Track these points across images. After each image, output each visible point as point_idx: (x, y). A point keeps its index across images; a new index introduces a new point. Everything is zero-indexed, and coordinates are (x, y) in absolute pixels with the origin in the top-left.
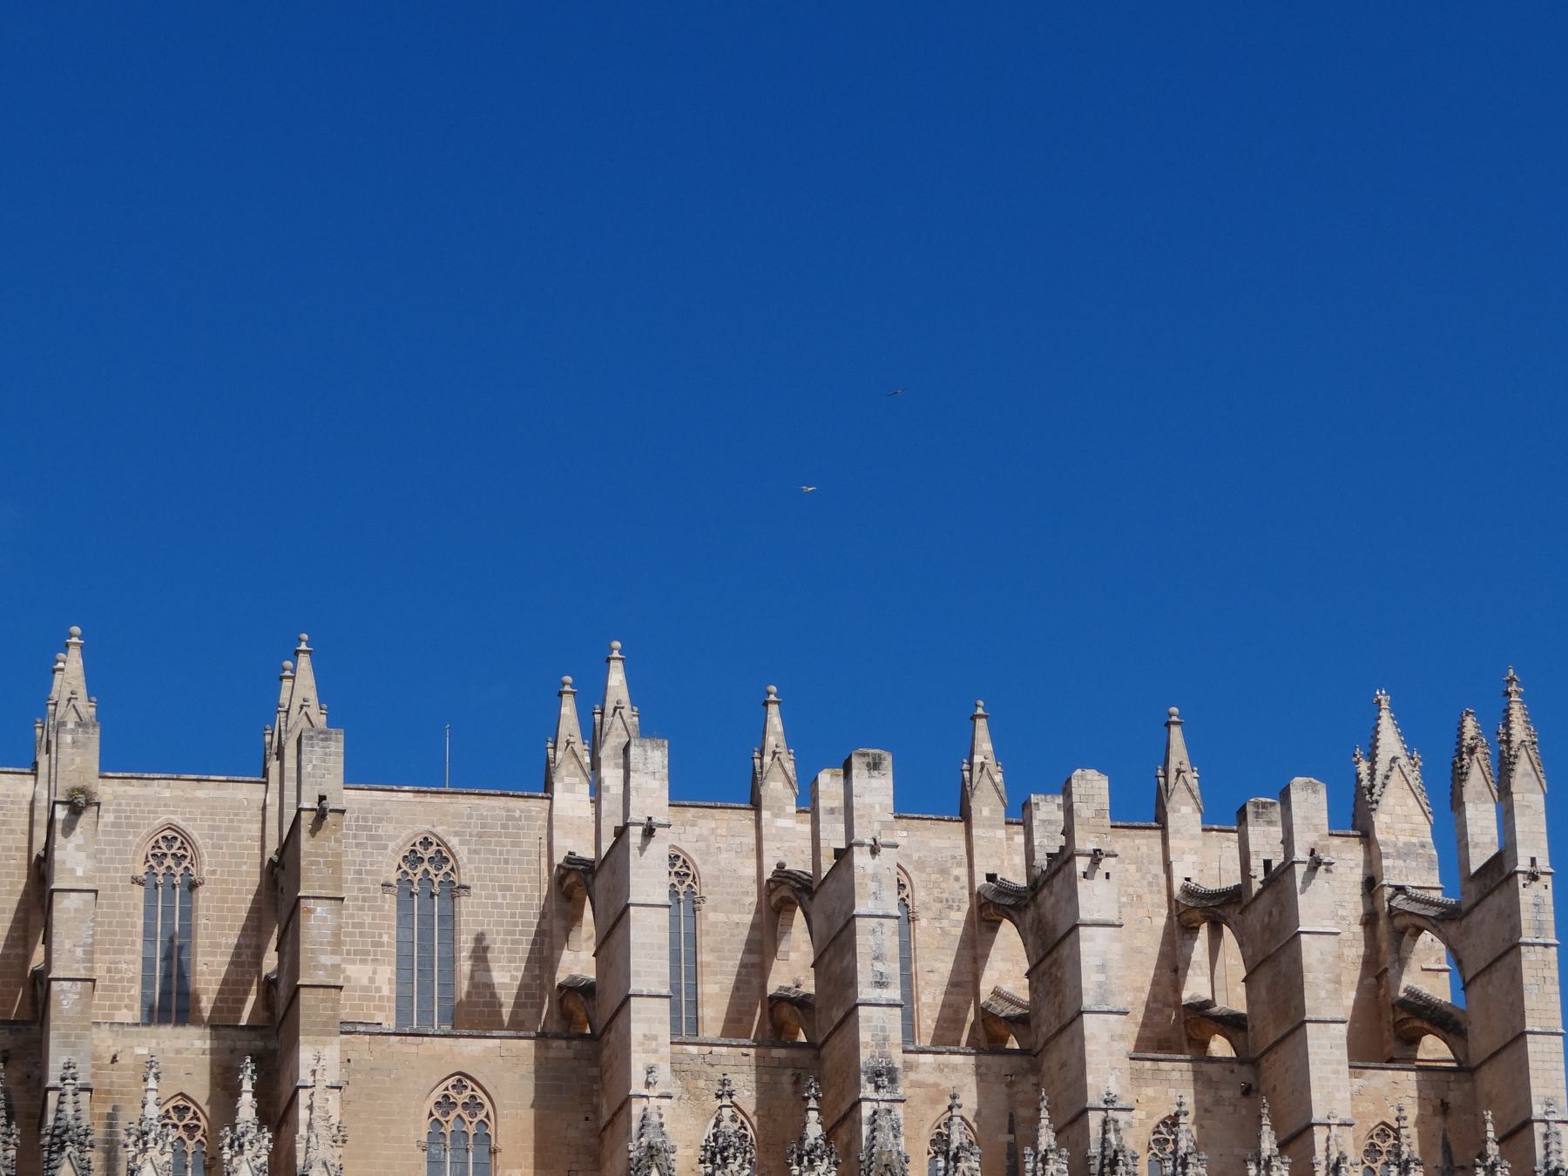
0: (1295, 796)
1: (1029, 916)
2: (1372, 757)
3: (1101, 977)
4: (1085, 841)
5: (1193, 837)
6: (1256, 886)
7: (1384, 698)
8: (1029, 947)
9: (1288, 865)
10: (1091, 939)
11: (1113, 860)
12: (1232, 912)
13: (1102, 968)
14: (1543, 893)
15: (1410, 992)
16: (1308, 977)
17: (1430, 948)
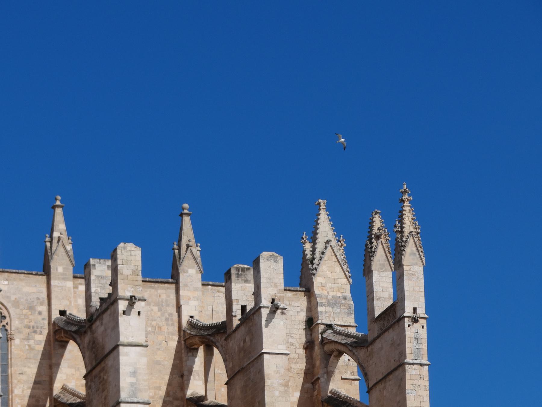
0: (263, 264)
1: (87, 339)
2: (314, 240)
3: (133, 380)
4: (125, 291)
5: (196, 290)
6: (236, 322)
7: (323, 203)
8: (86, 357)
9: (257, 309)
10: (127, 354)
11: (143, 303)
12: (220, 339)
13: (134, 374)
14: (421, 330)
15: (333, 392)
16: (268, 382)
17: (347, 365)
